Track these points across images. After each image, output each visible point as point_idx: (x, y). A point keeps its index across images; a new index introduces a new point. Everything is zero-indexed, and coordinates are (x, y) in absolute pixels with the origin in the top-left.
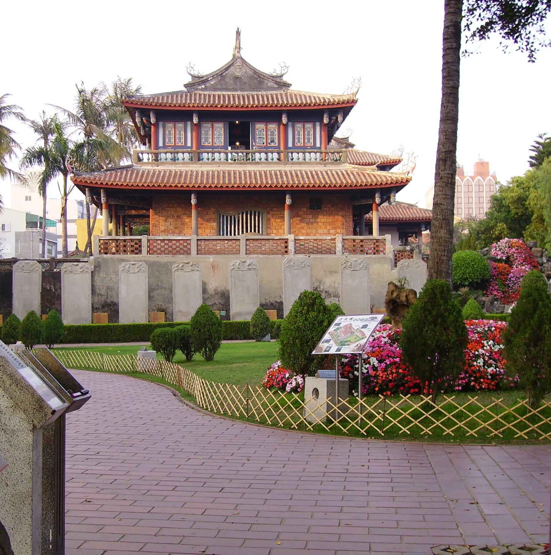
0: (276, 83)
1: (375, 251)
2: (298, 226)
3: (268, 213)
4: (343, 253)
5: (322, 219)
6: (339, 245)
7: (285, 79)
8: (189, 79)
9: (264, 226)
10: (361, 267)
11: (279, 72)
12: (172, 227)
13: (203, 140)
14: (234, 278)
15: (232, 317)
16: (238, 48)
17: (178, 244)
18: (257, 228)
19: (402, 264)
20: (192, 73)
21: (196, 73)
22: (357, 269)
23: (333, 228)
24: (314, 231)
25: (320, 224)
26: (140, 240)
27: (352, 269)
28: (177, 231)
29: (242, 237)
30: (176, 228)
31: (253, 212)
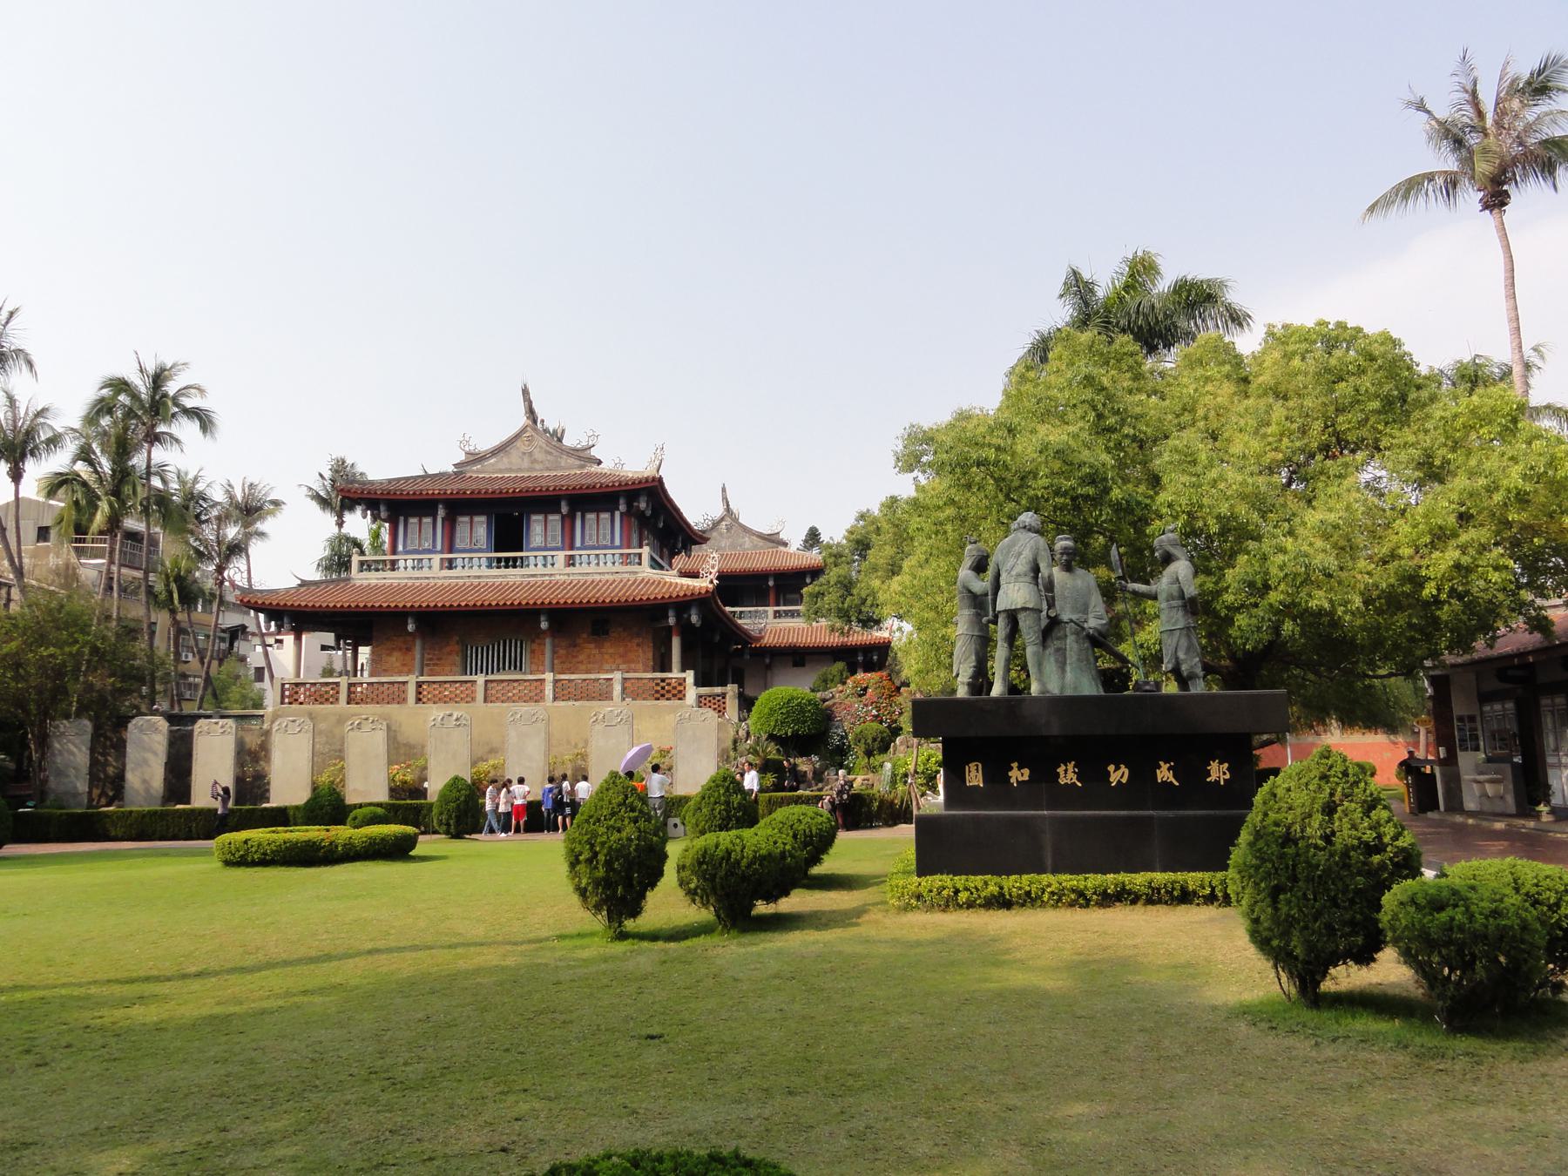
0: (580, 458)
1: (658, 695)
3: (533, 641)
4: (623, 699)
5: (609, 649)
6: (617, 688)
7: (594, 452)
8: (461, 457)
9: (528, 662)
11: (584, 444)
12: (398, 664)
13: (458, 541)
16: (531, 412)
17: (381, 689)
18: (518, 664)
20: (467, 449)
21: (472, 448)
23: (624, 663)
24: (596, 666)
25: (606, 657)
26: (337, 684)
28: (406, 669)
29: (480, 679)
30: (404, 665)
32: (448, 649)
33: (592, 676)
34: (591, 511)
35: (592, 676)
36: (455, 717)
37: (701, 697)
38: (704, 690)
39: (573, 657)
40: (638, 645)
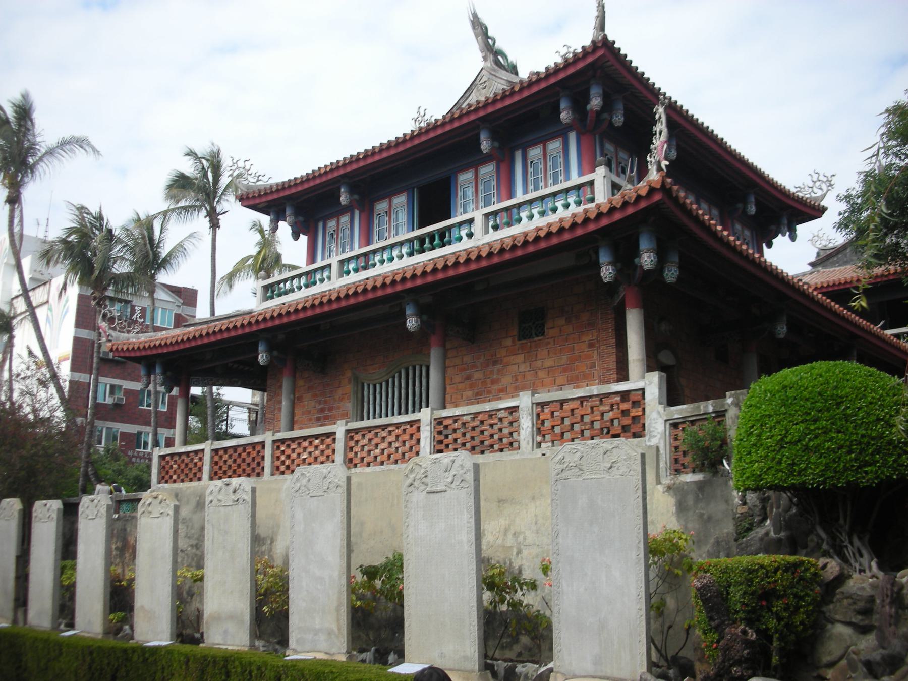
2: (496, 387)
6: (526, 424)
10: (450, 480)
14: (213, 526)
15: (206, 623)
19: (561, 461)
22: (439, 488)
25: (541, 374)
27: (429, 489)
29: (340, 429)
31: (417, 368)
32: (340, 392)
33: (487, 407)
34: (534, 144)
35: (487, 407)
36: (231, 488)
37: (675, 426)
38: (679, 411)
39: (494, 382)
40: (591, 345)
